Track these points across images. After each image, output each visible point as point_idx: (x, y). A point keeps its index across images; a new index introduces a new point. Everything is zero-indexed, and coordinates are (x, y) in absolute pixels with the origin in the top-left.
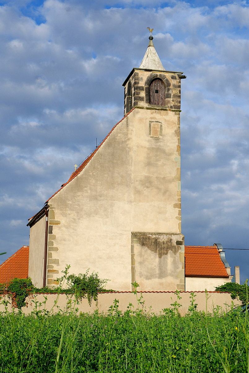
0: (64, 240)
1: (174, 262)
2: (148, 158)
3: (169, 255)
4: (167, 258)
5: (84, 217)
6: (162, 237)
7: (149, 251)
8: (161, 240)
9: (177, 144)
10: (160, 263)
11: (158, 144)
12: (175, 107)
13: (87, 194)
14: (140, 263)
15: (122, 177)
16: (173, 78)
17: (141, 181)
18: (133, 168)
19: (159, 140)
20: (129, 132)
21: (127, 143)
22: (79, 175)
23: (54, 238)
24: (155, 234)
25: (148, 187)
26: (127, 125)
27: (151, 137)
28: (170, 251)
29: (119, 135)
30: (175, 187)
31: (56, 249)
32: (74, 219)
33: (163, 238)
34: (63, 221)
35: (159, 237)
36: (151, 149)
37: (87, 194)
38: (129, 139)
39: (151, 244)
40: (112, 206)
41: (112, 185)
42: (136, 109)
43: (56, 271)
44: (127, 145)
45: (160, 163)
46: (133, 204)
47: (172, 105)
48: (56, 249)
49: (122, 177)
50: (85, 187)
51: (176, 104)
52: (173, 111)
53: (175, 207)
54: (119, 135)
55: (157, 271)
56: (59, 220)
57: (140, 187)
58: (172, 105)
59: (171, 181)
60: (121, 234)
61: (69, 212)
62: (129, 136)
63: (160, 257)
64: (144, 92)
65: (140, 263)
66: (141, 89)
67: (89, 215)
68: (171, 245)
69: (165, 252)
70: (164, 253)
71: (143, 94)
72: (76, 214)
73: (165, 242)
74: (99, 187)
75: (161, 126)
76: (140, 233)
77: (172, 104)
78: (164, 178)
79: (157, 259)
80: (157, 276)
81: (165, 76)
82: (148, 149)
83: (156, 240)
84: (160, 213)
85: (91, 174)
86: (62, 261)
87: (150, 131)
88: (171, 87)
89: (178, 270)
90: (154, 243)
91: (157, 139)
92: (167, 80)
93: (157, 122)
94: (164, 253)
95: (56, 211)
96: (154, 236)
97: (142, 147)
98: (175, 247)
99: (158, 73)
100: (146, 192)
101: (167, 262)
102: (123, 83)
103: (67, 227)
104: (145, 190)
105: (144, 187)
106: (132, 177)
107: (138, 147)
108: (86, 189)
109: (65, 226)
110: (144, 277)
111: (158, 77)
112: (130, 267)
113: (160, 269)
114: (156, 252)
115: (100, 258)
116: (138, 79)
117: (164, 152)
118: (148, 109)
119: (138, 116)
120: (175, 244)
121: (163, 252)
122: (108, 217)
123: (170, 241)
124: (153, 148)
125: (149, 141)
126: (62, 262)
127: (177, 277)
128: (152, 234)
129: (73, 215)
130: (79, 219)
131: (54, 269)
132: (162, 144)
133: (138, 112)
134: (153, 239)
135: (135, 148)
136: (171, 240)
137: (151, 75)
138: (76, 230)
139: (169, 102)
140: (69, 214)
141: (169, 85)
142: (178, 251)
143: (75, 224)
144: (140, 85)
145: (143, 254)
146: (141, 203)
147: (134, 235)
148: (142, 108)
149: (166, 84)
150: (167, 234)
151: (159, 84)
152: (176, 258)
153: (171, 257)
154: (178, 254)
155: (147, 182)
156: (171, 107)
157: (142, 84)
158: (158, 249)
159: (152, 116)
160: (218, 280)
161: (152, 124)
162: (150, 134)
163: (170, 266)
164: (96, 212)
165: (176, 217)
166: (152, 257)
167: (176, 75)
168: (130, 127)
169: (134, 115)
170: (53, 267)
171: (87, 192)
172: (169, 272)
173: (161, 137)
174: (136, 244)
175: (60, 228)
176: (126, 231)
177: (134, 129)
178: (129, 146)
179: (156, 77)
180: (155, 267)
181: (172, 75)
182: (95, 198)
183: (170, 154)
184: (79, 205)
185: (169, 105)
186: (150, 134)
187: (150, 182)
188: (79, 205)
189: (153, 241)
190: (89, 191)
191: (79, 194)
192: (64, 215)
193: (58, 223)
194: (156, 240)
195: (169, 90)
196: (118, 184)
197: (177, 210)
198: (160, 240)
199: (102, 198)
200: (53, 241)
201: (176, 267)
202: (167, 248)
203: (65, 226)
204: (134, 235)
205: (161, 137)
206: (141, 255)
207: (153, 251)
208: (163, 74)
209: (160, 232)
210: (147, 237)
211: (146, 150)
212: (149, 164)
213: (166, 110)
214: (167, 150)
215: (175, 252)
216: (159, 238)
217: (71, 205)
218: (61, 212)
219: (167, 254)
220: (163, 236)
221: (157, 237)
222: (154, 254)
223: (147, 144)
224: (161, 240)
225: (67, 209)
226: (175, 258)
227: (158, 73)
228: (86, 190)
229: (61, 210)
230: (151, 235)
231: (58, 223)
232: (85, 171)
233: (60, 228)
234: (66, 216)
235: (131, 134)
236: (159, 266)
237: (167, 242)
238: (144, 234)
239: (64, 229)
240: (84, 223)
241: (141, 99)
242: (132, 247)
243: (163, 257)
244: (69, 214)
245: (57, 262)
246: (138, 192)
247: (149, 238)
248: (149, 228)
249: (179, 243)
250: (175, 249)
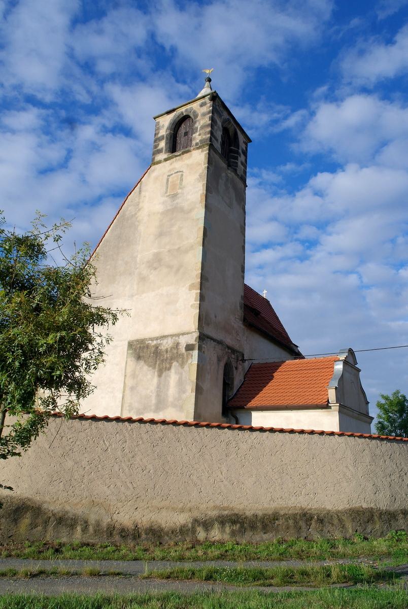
1: (180, 383)
3: (173, 370)
4: (169, 376)
6: (164, 342)
7: (146, 368)
8: (164, 346)
10: (158, 386)
11: (175, 202)
17: (148, 262)
19: (178, 196)
21: (137, 216)
24: (157, 339)
26: (140, 191)
28: (175, 364)
33: (167, 343)
35: (162, 342)
36: (165, 213)
39: (150, 356)
44: (137, 218)
45: (175, 229)
46: (134, 298)
47: (198, 141)
51: (204, 137)
53: (190, 289)
55: (154, 401)
58: (198, 141)
62: (141, 205)
63: (160, 376)
64: (165, 140)
65: (132, 389)
68: (177, 353)
69: (168, 366)
70: (166, 367)
71: (162, 144)
73: (169, 349)
75: (182, 175)
76: (137, 341)
79: (156, 380)
80: (153, 407)
81: (191, 109)
82: (163, 213)
83: (157, 347)
89: (184, 396)
90: (153, 353)
93: (177, 172)
94: (166, 367)
96: (155, 342)
98: (183, 355)
101: (168, 383)
104: (151, 274)
105: (151, 270)
106: (138, 259)
110: (134, 412)
111: (184, 114)
113: (158, 396)
114: (154, 368)
117: (182, 210)
120: (183, 350)
121: (165, 367)
123: (177, 346)
127: (181, 408)
139: (195, 138)
142: (187, 361)
144: (160, 135)
145: (137, 373)
150: (172, 336)
152: (184, 373)
153: (176, 373)
154: (186, 368)
155: (156, 262)
157: (163, 132)
158: (158, 363)
159: (171, 167)
160: (277, 413)
162: (166, 193)
163: (172, 391)
165: (192, 306)
166: (149, 376)
168: (143, 193)
169: (149, 176)
172: (171, 399)
173: (180, 191)
174: (130, 359)
176: (121, 341)
179: (182, 116)
180: (151, 394)
181: (201, 102)
183: (190, 211)
186: (166, 193)
189: (153, 349)
194: (157, 347)
198: (162, 347)
201: (182, 391)
202: (172, 359)
205: (180, 191)
206: (134, 376)
207: (150, 366)
208: (189, 107)
209: (166, 334)
210: (145, 345)
214: (186, 205)
215: (182, 365)
216: (162, 344)
219: (169, 369)
220: (167, 340)
221: (159, 342)
222: (151, 372)
224: (164, 346)
226: (181, 374)
230: (150, 342)
235: (143, 202)
236: (157, 391)
237: (171, 349)
241: (160, 151)
243: (164, 374)
246: (143, 279)
247: (148, 347)
249: (189, 348)
250: (183, 358)
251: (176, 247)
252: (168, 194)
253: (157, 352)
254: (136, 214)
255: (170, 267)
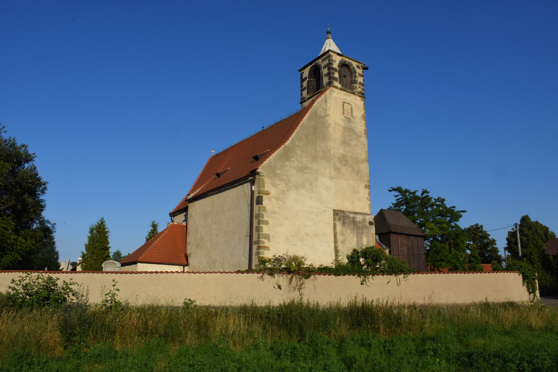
0: (275, 213)
2: (344, 136)
3: (364, 235)
5: (293, 189)
7: (349, 231)
9: (364, 127)
11: (350, 124)
12: (361, 93)
13: (294, 165)
14: (343, 242)
15: (324, 151)
16: (358, 67)
17: (339, 158)
18: (332, 145)
20: (328, 108)
22: (286, 144)
23: (265, 209)
25: (344, 165)
27: (345, 117)
29: (320, 109)
30: (365, 168)
31: (267, 223)
32: (283, 190)
34: (273, 191)
37: (294, 165)
38: (328, 115)
40: (316, 180)
41: (315, 158)
42: (332, 88)
43: (267, 247)
44: (327, 120)
48: (267, 223)
49: (324, 151)
50: (293, 157)
52: (360, 96)
54: (320, 109)
56: (269, 190)
57: (338, 164)
59: (362, 162)
60: (325, 211)
61: (278, 182)
62: (328, 112)
65: (343, 242)
66: (335, 70)
67: (297, 187)
71: (336, 75)
72: (284, 185)
74: (304, 159)
75: (352, 108)
77: (359, 90)
78: (356, 158)
79: (355, 239)
82: (343, 128)
84: (355, 192)
85: (297, 144)
86: (273, 237)
87: (344, 111)
88: (357, 74)
91: (349, 119)
92: (354, 67)
95: (266, 180)
96: (352, 216)
97: (338, 125)
99: (347, 60)
100: (343, 169)
102: (299, 69)
103: (277, 199)
107: (335, 124)
108: (293, 159)
109: (274, 197)
112: (333, 245)
115: (307, 235)
116: (332, 60)
117: (355, 132)
118: (341, 89)
119: (334, 95)
122: (313, 192)
124: (347, 128)
125: (343, 120)
126: (273, 237)
128: (350, 212)
129: (282, 186)
130: (288, 191)
131: (265, 245)
132: (353, 125)
133: (334, 91)
134: (352, 217)
135: (333, 125)
136: (365, 219)
137: (342, 59)
138: (285, 203)
139: (356, 88)
140: (279, 185)
141: (355, 72)
143: (284, 196)
146: (339, 181)
147: (336, 213)
148: (336, 88)
149: (353, 71)
150: (361, 214)
151: (346, 70)
155: (343, 160)
156: (358, 93)
157: (335, 65)
161: (345, 105)
162: (344, 114)
164: (303, 186)
166: (351, 236)
167: (360, 65)
168: (328, 104)
170: (264, 243)
171: (294, 163)
173: (352, 118)
175: (270, 199)
177: (331, 107)
178: (328, 122)
182: (302, 170)
183: (360, 136)
184: (287, 176)
185: (357, 90)
186: (344, 114)
187: (346, 161)
188: (287, 176)
189: (352, 219)
190: (296, 162)
191: (287, 163)
192: (274, 185)
193: (268, 193)
194: (354, 218)
195: (355, 76)
196: (321, 159)
197: (367, 190)
199: (307, 171)
200: (263, 213)
202: (363, 228)
203: (274, 197)
204: (336, 213)
205: (352, 118)
206: (342, 234)
208: (350, 61)
209: (356, 211)
211: (342, 129)
212: (345, 143)
213: (354, 94)
217: (280, 174)
218: (271, 181)
219: (362, 234)
223: (341, 123)
225: (277, 178)
227: (347, 60)
228: (293, 161)
229: (271, 179)
231: (268, 193)
232: (292, 140)
233: (270, 199)
234: (275, 187)
238: (343, 212)
239: (273, 200)
240: (292, 195)
241: (336, 79)
242: (335, 225)
244: (279, 185)
245: (267, 237)
246: (337, 169)
247: (348, 217)
248: (346, 206)
249: (371, 223)
251: (355, 157)
252: (345, 115)
253: (354, 222)
254: (325, 117)
255: (352, 167)
